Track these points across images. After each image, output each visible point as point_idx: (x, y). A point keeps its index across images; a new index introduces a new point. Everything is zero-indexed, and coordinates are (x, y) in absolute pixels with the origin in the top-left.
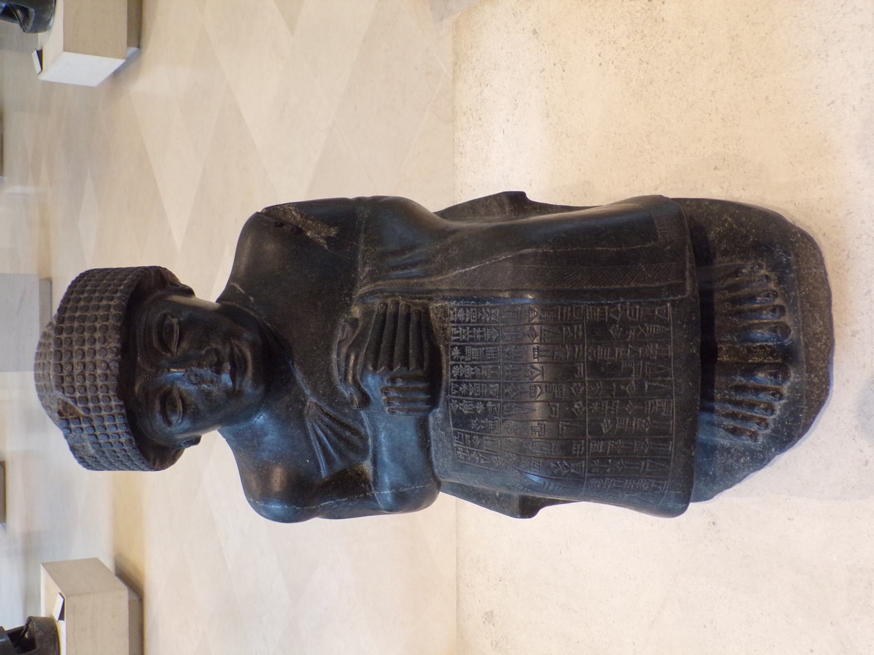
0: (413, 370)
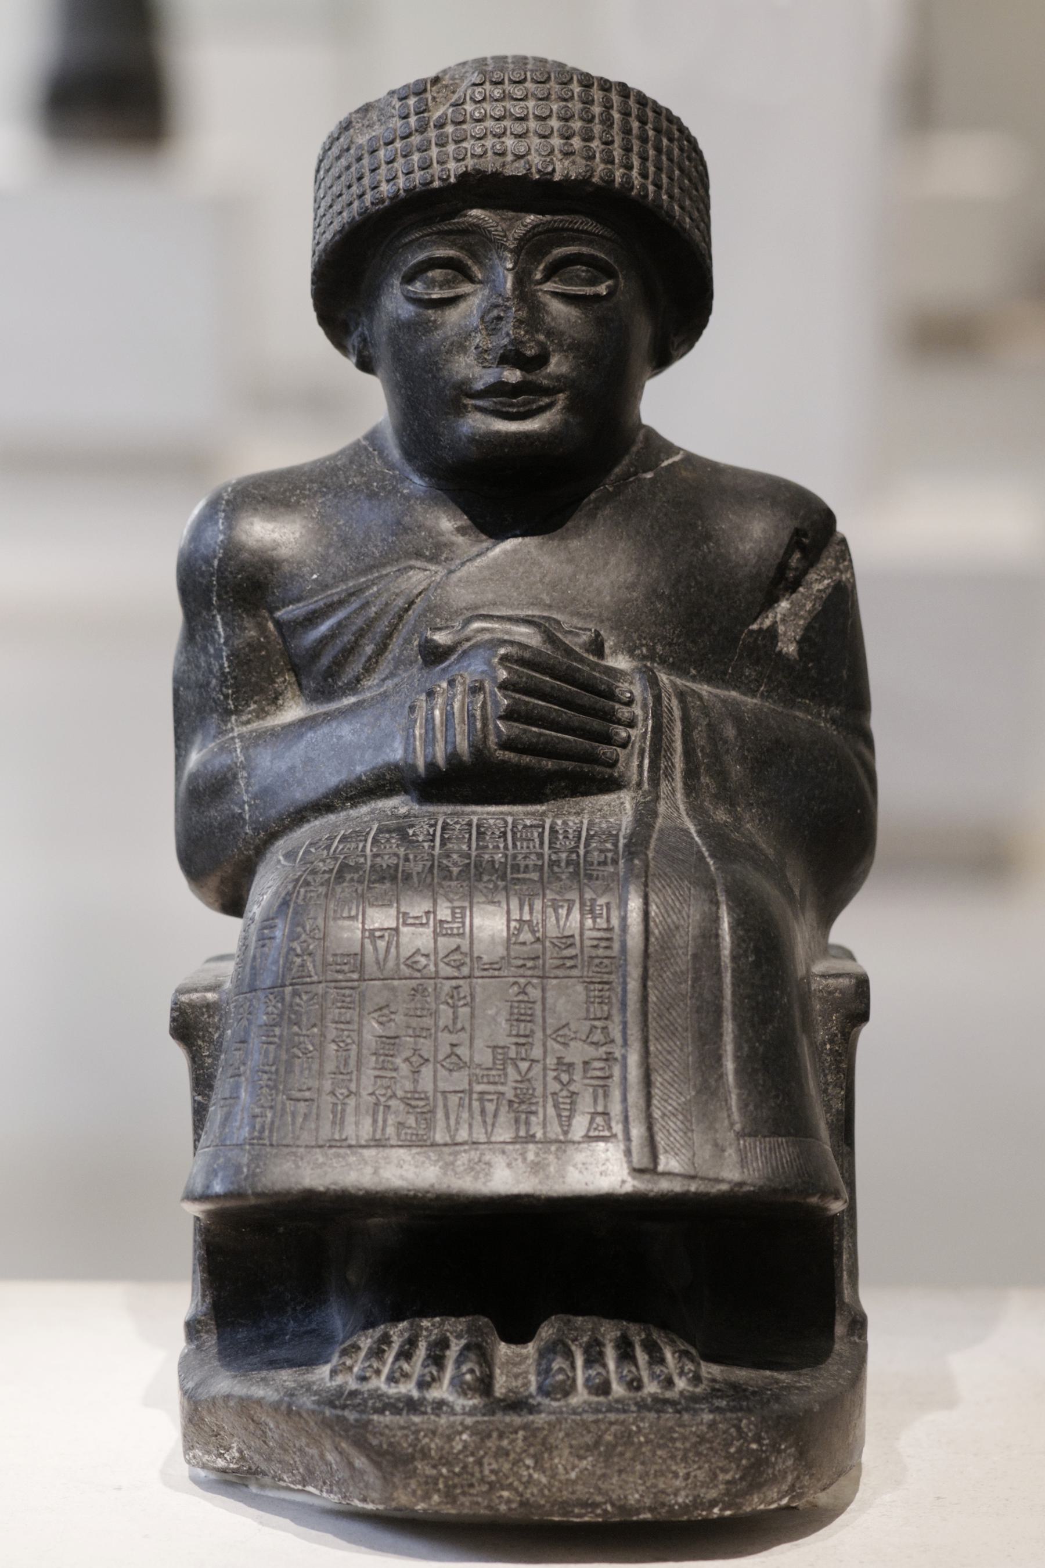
0: (497, 727)
